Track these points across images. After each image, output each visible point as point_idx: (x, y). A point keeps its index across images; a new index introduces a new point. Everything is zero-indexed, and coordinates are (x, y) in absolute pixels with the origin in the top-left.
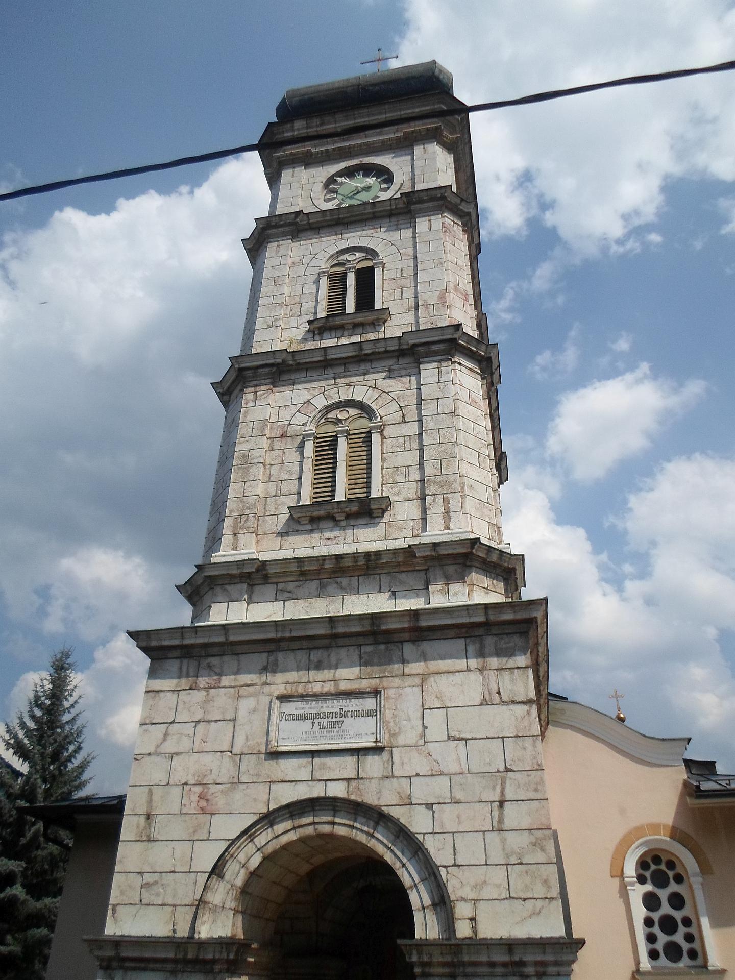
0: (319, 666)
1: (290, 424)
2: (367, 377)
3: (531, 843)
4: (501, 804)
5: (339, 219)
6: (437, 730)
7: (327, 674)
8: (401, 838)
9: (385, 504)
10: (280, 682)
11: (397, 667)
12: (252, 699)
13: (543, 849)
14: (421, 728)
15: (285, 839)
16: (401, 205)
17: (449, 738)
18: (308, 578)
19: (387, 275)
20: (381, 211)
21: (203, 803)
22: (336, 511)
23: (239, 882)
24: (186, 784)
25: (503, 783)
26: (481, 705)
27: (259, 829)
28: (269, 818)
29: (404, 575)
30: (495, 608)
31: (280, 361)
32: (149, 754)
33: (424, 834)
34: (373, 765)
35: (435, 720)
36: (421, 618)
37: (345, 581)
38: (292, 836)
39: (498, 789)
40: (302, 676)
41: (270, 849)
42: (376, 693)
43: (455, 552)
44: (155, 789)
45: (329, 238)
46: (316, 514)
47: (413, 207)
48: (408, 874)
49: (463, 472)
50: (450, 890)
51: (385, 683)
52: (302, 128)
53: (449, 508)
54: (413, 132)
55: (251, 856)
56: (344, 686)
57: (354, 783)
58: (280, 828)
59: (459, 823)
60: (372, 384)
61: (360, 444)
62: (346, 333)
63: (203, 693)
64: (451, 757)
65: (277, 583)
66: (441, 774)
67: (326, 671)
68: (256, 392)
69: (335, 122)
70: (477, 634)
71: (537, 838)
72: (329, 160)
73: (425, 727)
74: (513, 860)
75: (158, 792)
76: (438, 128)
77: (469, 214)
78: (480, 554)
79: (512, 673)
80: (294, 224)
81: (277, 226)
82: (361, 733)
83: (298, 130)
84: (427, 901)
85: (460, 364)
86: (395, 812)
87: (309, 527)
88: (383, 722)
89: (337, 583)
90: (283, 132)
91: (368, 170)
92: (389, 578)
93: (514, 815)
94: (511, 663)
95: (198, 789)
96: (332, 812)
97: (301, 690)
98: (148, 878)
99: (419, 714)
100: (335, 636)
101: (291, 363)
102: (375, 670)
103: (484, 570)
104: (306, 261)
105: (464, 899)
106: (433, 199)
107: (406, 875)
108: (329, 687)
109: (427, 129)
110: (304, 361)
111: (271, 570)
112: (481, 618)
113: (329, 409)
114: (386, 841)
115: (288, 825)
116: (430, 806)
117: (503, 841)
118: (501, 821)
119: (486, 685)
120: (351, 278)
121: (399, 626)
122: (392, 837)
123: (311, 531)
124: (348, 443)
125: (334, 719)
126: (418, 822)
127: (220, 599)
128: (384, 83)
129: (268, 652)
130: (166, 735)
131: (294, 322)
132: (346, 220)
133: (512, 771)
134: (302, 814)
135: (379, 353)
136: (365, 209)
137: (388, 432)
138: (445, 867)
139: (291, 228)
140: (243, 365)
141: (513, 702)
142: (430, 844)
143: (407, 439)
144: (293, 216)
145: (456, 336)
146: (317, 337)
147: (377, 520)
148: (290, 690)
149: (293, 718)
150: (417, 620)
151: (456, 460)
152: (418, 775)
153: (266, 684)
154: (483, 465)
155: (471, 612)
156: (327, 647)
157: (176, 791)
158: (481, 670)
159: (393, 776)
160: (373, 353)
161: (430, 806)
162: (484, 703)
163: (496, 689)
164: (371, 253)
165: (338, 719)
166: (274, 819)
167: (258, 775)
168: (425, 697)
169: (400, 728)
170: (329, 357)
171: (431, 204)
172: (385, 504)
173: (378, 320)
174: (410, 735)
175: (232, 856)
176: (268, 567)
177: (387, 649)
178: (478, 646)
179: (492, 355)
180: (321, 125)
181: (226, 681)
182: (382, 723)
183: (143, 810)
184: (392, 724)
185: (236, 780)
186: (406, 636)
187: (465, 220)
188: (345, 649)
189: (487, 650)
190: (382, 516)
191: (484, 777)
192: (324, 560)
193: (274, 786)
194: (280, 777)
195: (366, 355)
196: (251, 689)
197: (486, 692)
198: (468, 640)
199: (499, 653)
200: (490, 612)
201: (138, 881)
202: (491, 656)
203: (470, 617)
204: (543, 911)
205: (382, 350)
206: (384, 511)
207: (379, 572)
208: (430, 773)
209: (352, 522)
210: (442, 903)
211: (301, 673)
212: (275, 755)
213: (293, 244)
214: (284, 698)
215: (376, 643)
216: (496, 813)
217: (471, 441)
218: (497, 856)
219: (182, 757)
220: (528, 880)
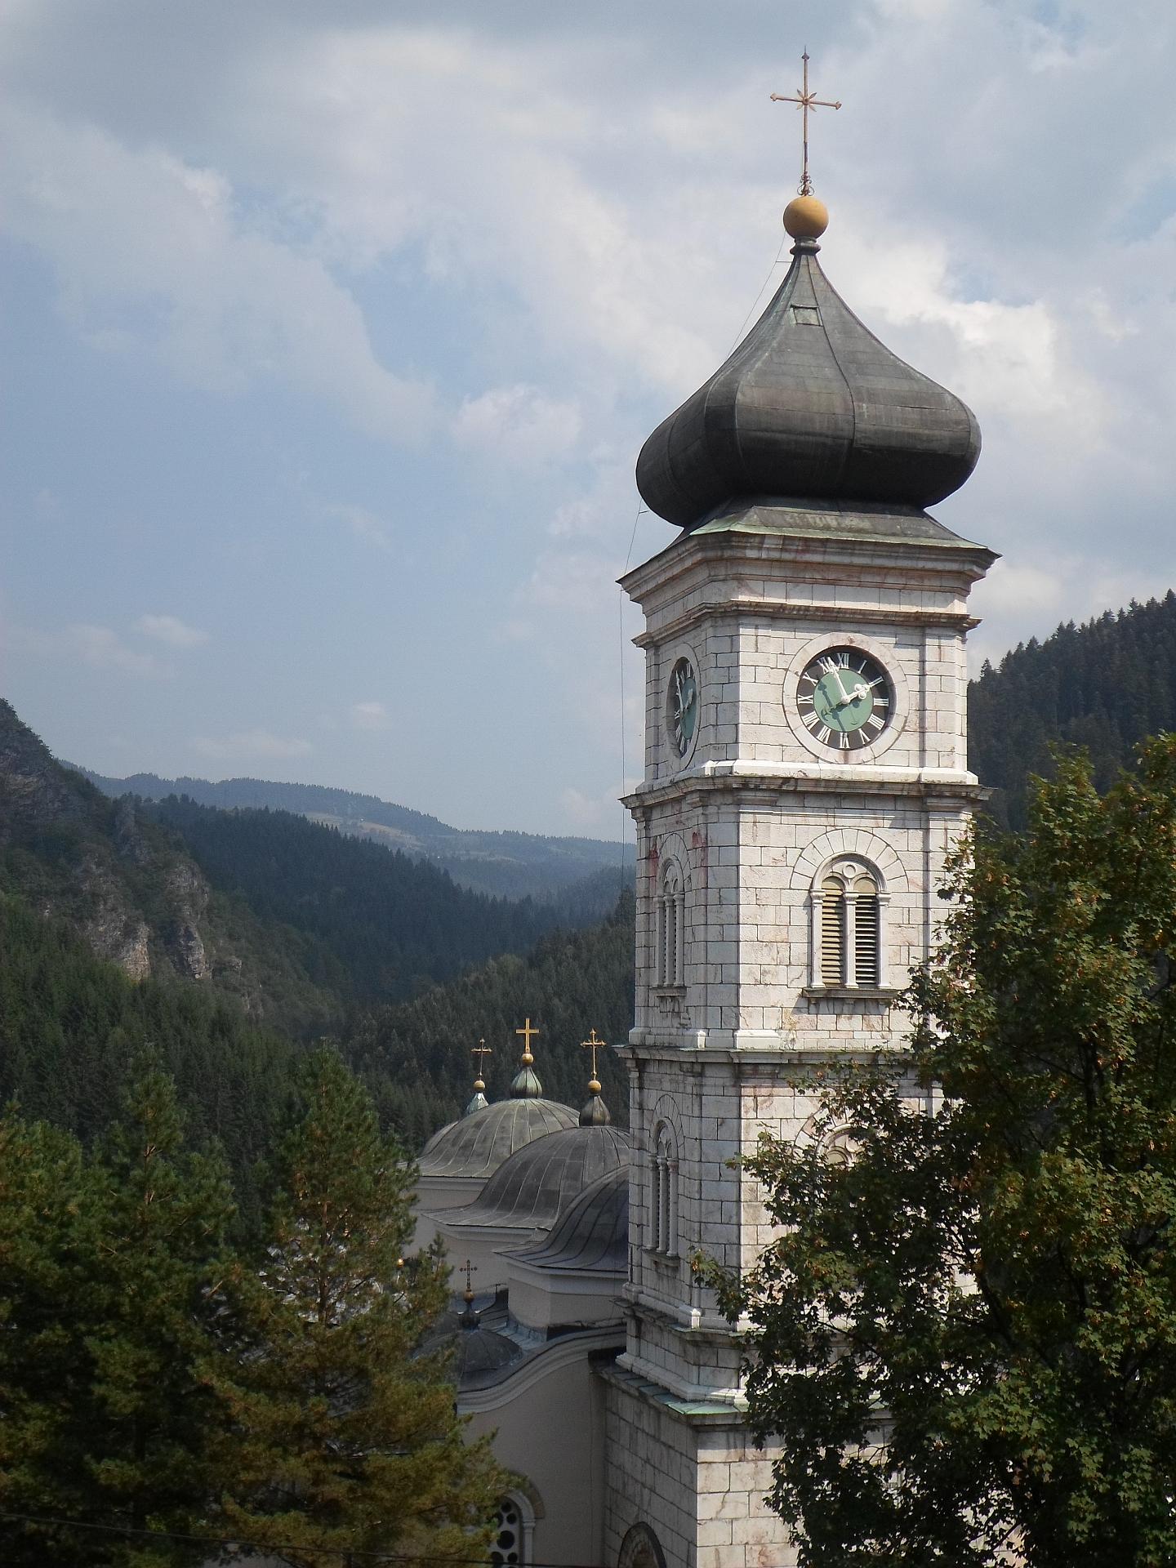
21: (763, 1559)
44: (721, 1549)
47: (931, 802)
54: (932, 615)
62: (846, 1008)
63: (752, 1465)
69: (825, 553)
75: (724, 1551)
81: (757, 789)
90: (745, 548)
95: (758, 1548)
106: (954, 796)
120: (851, 911)
130: (723, 1502)
131: (782, 975)
146: (812, 1007)
164: (874, 873)
180: (804, 551)
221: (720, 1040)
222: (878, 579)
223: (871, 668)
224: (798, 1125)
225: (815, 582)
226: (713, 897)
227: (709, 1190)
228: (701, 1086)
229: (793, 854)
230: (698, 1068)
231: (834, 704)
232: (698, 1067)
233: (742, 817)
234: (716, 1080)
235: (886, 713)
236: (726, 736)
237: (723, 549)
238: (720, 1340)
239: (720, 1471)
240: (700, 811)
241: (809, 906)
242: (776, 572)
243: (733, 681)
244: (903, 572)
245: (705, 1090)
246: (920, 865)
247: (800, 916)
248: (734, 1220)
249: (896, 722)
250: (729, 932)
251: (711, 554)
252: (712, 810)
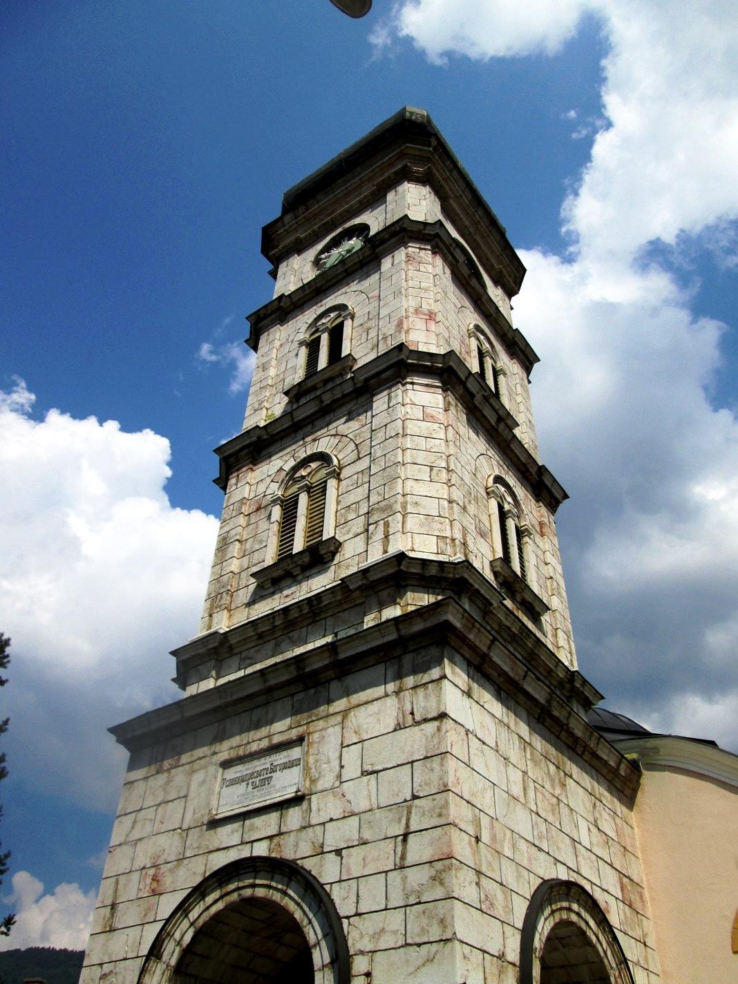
0: (257, 726)
1: (265, 496)
2: (330, 427)
3: (431, 877)
4: (405, 836)
5: (317, 288)
6: (352, 770)
7: (264, 731)
8: (309, 891)
9: (335, 546)
10: (225, 750)
12: (202, 771)
13: (442, 884)
14: (338, 768)
15: (214, 910)
16: (368, 253)
17: (362, 774)
18: (265, 640)
19: (357, 322)
20: (351, 266)
21: (155, 885)
22: (291, 566)
23: (173, 962)
24: (144, 868)
25: (409, 813)
26: (395, 730)
27: (193, 902)
28: (200, 891)
29: (346, 613)
30: (404, 621)
31: (255, 439)
32: (120, 845)
33: (331, 884)
34: (294, 816)
35: (351, 755)
36: (339, 650)
37: (295, 634)
38: (220, 906)
39: (404, 821)
40: (245, 738)
41: (200, 922)
42: (300, 740)
43: (384, 574)
45: (311, 310)
46: (275, 575)
47: (377, 250)
48: (313, 932)
49: (408, 490)
50: (350, 943)
51: (312, 728)
52: (292, 220)
53: (388, 532)
54: (383, 181)
55: (184, 933)
56: (276, 739)
57: (275, 840)
58: (210, 899)
59: (365, 866)
60: (333, 432)
61: (320, 494)
64: (361, 794)
65: (241, 653)
66: (353, 814)
67: (263, 729)
68: (238, 476)
69: (318, 202)
70: (395, 655)
71: (437, 871)
72: (319, 238)
73: (342, 767)
74: (412, 900)
76: (405, 167)
77: (437, 235)
78: (413, 570)
79: (427, 688)
80: (280, 308)
81: (266, 316)
82: (286, 784)
83: (288, 223)
84: (327, 959)
85: (412, 383)
87: (271, 590)
88: (307, 769)
89: (289, 638)
90: (277, 231)
91: (349, 234)
92: (333, 620)
93: (419, 849)
94: (426, 678)
96: (253, 874)
97: (241, 753)
98: (106, 968)
99: (338, 754)
100: (270, 690)
101: (265, 437)
102: (303, 718)
103: (424, 587)
104: (290, 339)
105: (362, 953)
107: (311, 932)
108: (264, 744)
109: (396, 173)
110: (275, 432)
111: (233, 640)
112: (392, 636)
113: (295, 469)
114: (296, 897)
115: (215, 895)
116: (338, 852)
117: (404, 879)
118: (403, 857)
119: (401, 709)
121: (320, 664)
122: (302, 891)
123: (273, 593)
124: (309, 497)
125: (265, 776)
126: (327, 871)
127: (193, 680)
129: (219, 721)
132: (324, 288)
133: (418, 797)
134: (229, 881)
135: (339, 399)
136: (337, 270)
137: (345, 473)
138: (348, 917)
139: (278, 314)
140: (226, 454)
141: (426, 720)
142: (337, 894)
143: (360, 475)
144: (277, 302)
145: (401, 357)
147: (328, 565)
148: (233, 754)
149: (233, 782)
150: (336, 653)
151: (400, 481)
152: (331, 820)
153: (215, 753)
154: (435, 478)
155: (382, 631)
156: (266, 704)
159: (310, 826)
160: (334, 402)
161: (338, 852)
162: (399, 727)
163: (408, 708)
165: (269, 775)
166: (205, 891)
167: (199, 847)
168: (345, 735)
169: (320, 773)
170: (296, 420)
171: (392, 241)
172: (335, 546)
173: (344, 369)
175: (168, 934)
176: (230, 638)
177: (316, 692)
178: (396, 667)
179: (452, 364)
180: (307, 210)
182: (307, 769)
184: (313, 770)
185: (181, 857)
186: (330, 673)
187: (434, 242)
188: (281, 701)
189: (404, 670)
190: (333, 559)
191: (390, 810)
192: (274, 618)
194: (216, 845)
195: (328, 405)
196: (202, 762)
197: (401, 715)
198: (388, 663)
199: (414, 672)
200: (401, 626)
202: (408, 675)
203: (383, 637)
204: (437, 957)
205: (340, 395)
206: (334, 554)
207: (324, 616)
208: (342, 816)
209: (307, 574)
211: (243, 735)
212: (214, 824)
213: (281, 328)
214: (226, 765)
215: (307, 688)
216: (399, 849)
217: (421, 457)
218: (396, 899)
219: (144, 841)
220: (425, 921)
224: (269, 480)
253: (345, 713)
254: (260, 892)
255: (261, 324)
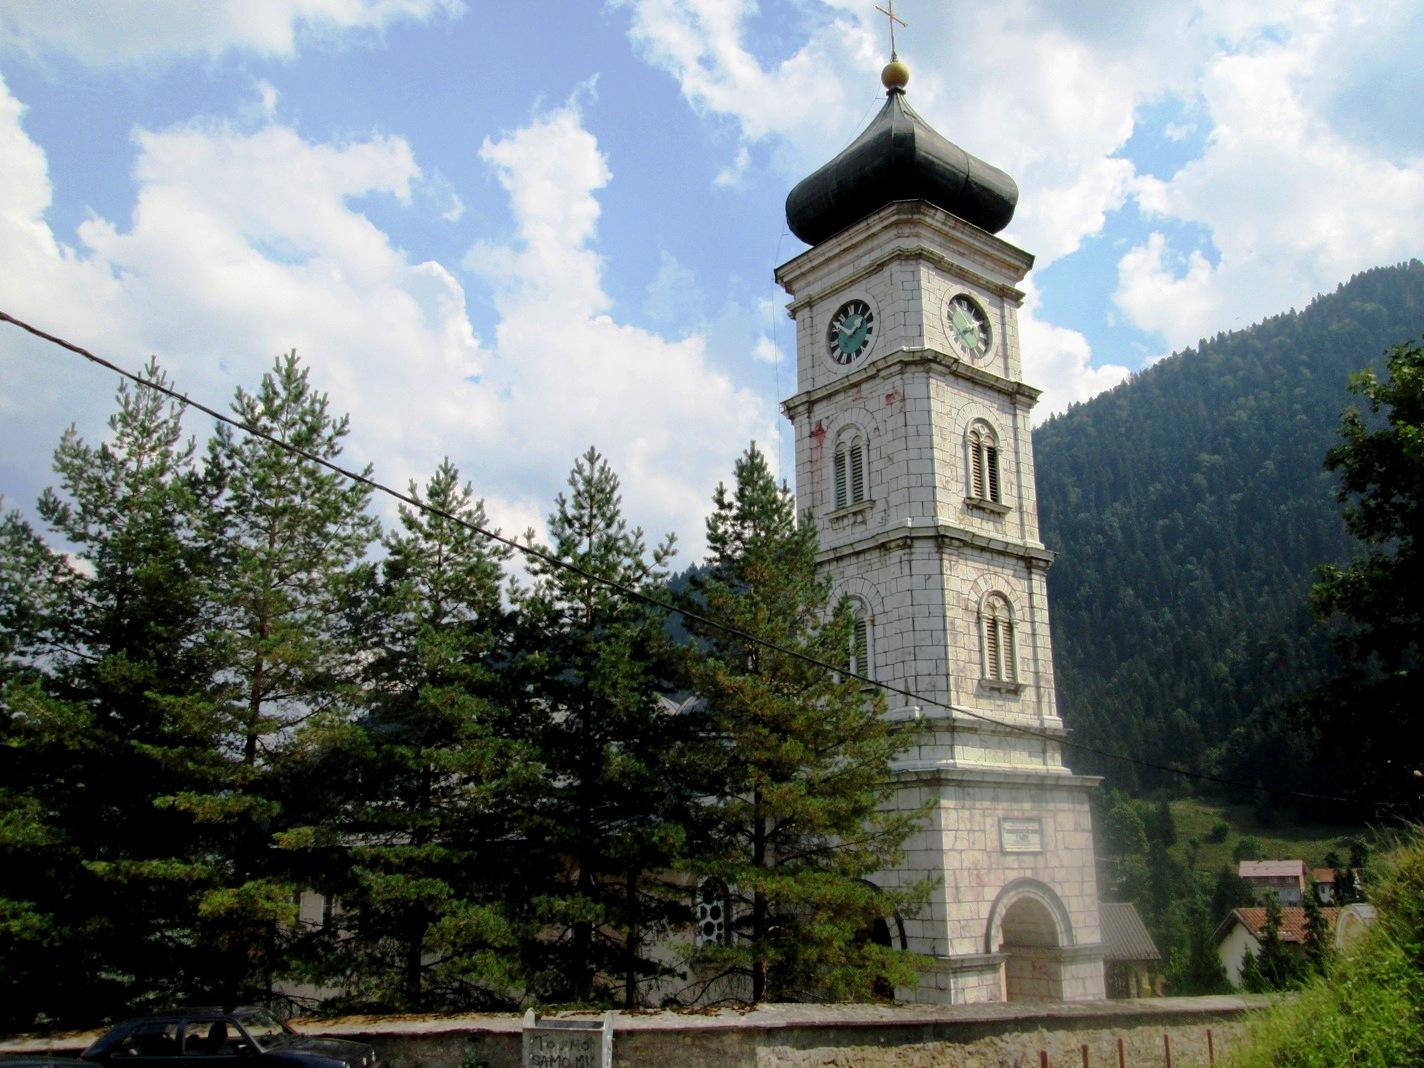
0: (1015, 800)
4: (1083, 882)
6: (1060, 845)
11: (1044, 805)
38: (1015, 899)
47: (1018, 396)
56: (1027, 814)
63: (968, 812)
81: (940, 363)
86: (1051, 885)
87: (987, 694)
90: (925, 215)
95: (975, 872)
108: (1020, 814)
123: (989, 697)
128: (984, 189)
130: (956, 838)
149: (1010, 832)
157: (966, 873)
158: (1074, 811)
162: (1075, 830)
164: (993, 434)
174: (1051, 847)
180: (953, 228)
181: (978, 804)
183: (953, 884)
193: (1007, 872)
201: (957, 925)
210: (1069, 929)
221: (928, 522)
222: (982, 260)
223: (979, 314)
225: (954, 251)
226: (911, 430)
227: (920, 624)
228: (911, 554)
229: (955, 411)
230: (909, 541)
231: (961, 330)
232: (908, 542)
233: (931, 380)
234: (923, 549)
235: (987, 343)
236: (913, 331)
237: (913, 213)
238: (941, 723)
239: (953, 814)
240: (899, 377)
241: (965, 446)
242: (937, 238)
243: (920, 298)
244: (994, 260)
245: (914, 557)
246: (1012, 435)
247: (960, 453)
248: (942, 643)
249: (993, 348)
250: (926, 453)
251: (903, 217)
252: (906, 375)
253: (1055, 812)
254: (1032, 896)
255: (934, 366)
